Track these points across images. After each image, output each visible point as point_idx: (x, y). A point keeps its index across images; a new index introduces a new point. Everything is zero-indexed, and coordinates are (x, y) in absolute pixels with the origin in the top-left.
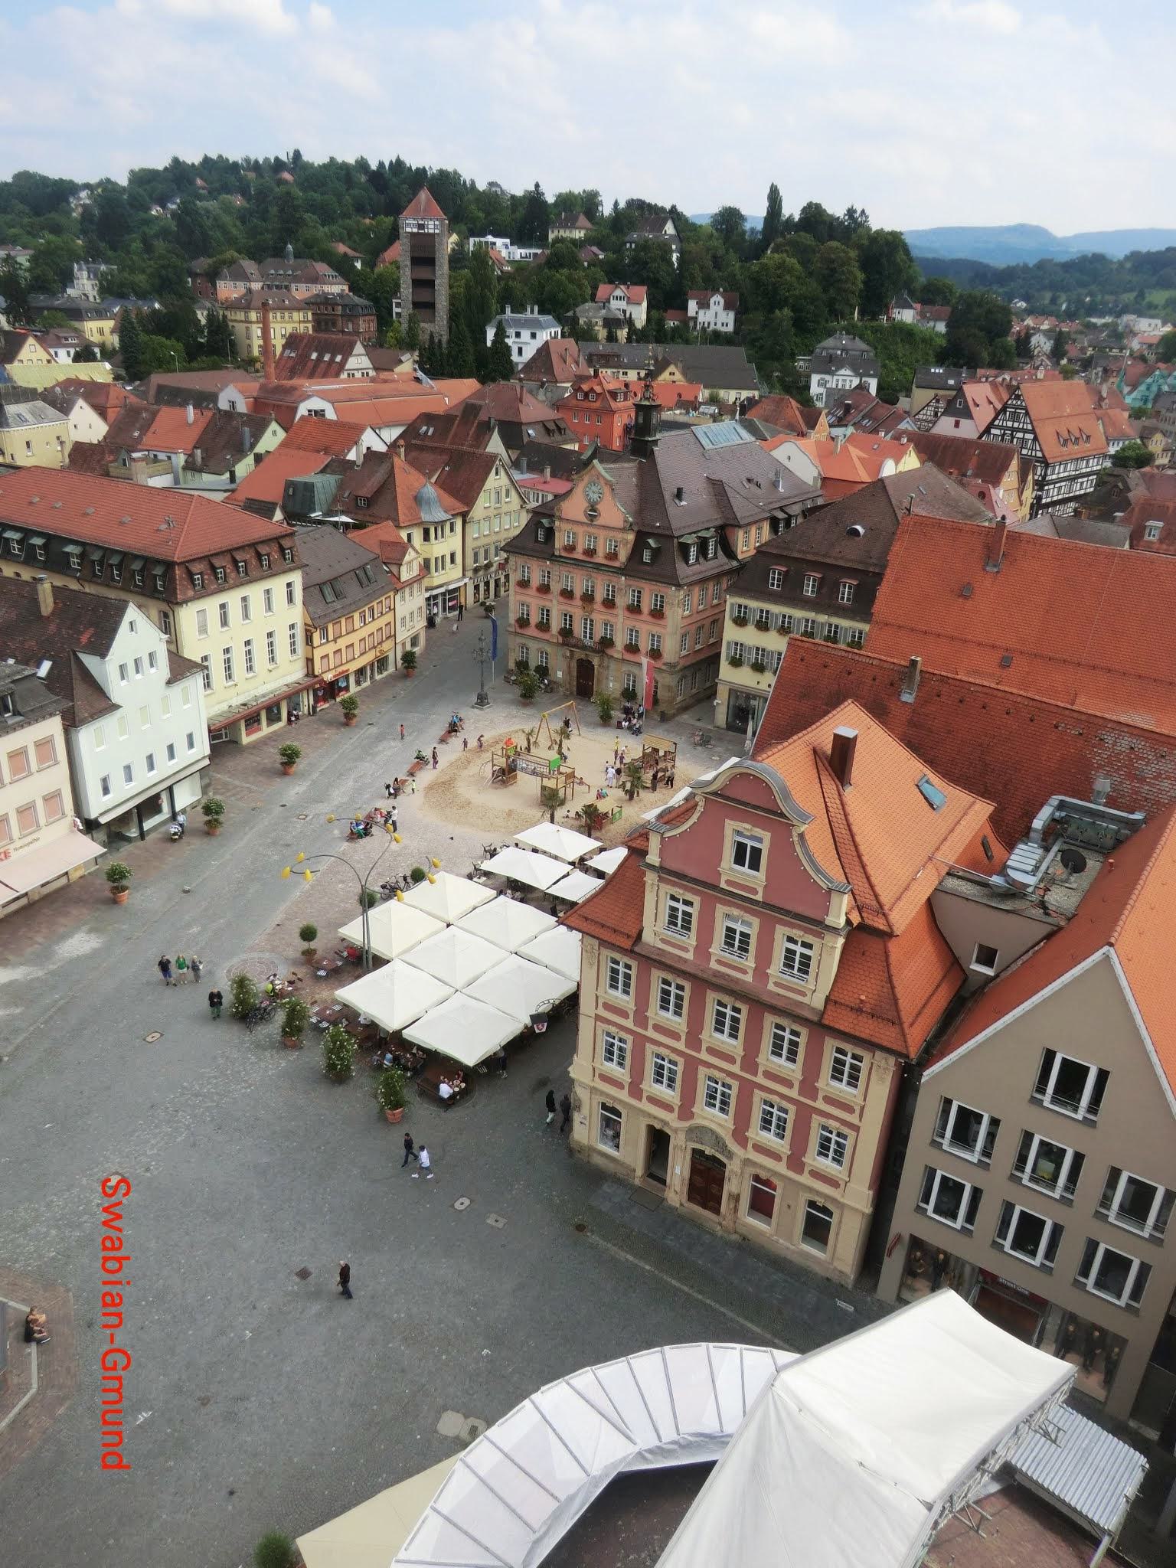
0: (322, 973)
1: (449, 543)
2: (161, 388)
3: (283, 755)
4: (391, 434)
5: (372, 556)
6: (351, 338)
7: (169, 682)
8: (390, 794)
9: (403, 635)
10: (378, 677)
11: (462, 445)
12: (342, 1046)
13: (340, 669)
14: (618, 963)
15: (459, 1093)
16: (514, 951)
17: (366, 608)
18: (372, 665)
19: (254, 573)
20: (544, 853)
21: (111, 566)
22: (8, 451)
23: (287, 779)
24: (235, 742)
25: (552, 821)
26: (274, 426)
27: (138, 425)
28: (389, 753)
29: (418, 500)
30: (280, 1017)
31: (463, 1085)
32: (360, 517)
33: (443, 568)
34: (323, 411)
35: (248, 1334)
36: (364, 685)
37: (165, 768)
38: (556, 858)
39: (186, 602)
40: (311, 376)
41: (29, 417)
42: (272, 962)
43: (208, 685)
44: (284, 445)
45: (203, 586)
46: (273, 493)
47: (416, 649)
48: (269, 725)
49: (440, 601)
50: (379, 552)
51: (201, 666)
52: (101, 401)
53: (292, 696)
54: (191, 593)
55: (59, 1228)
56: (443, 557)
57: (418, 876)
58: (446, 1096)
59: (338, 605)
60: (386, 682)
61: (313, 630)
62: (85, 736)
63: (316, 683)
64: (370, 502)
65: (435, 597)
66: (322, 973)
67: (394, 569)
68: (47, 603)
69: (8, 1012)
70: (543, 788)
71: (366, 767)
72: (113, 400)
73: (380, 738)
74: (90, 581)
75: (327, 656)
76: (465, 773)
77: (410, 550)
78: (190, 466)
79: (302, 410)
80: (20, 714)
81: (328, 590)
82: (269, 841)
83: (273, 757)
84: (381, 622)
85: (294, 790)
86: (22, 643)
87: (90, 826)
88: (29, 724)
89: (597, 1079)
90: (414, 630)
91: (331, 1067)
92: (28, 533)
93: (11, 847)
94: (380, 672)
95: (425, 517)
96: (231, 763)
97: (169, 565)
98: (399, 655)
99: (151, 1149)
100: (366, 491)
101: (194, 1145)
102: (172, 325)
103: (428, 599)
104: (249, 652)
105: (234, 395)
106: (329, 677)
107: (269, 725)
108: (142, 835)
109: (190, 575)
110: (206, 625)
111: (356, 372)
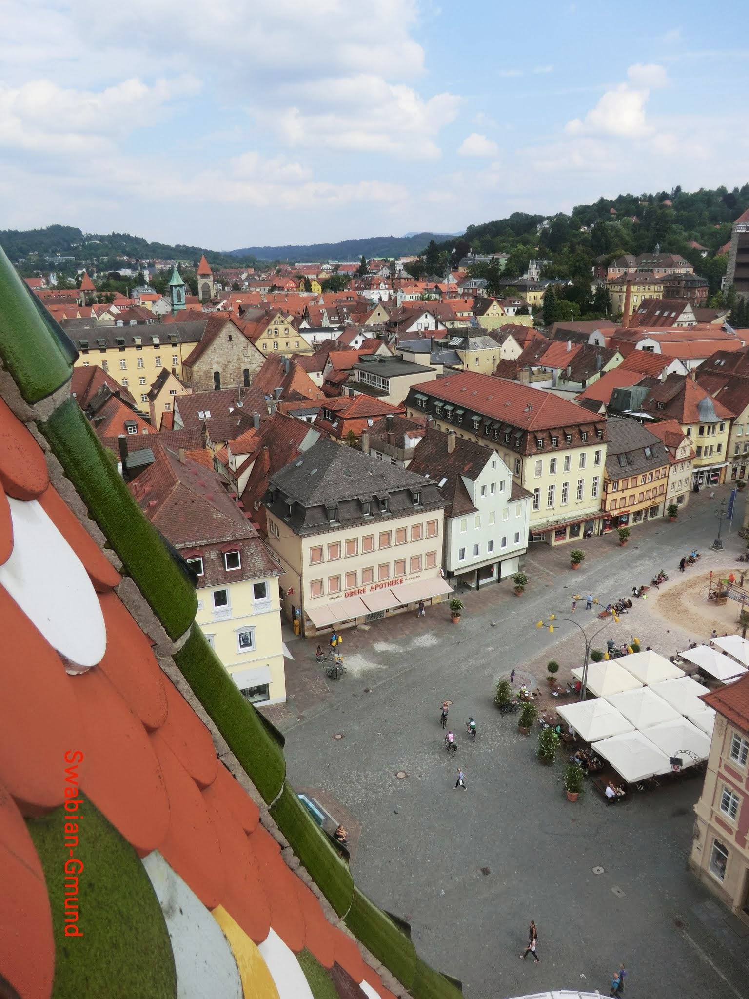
0: (556, 694)
1: (719, 437)
2: (559, 330)
3: (573, 556)
4: (695, 364)
5: (660, 441)
6: (684, 302)
7: (510, 500)
8: (635, 594)
9: (672, 494)
10: (649, 519)
11: (744, 374)
12: (550, 741)
13: (623, 510)
14: (740, 740)
15: (619, 797)
16: (685, 714)
17: (648, 473)
18: (646, 510)
19: (575, 443)
20: (732, 657)
21: (494, 430)
22: (466, 363)
23: (572, 572)
24: (547, 544)
25: (744, 636)
26: (618, 355)
27: (538, 351)
28: (642, 568)
29: (699, 407)
30: (520, 714)
31: (623, 793)
32: (658, 415)
33: (705, 455)
34: (653, 347)
35: (443, 892)
36: (639, 522)
37: (499, 550)
38: (739, 662)
39: (531, 455)
40: (654, 325)
41: (480, 345)
42: (529, 680)
43: (536, 506)
44: (621, 367)
45: (543, 447)
46: (604, 396)
47: (680, 506)
48: (570, 537)
49: (705, 475)
50: (663, 438)
51: (527, 494)
52: (522, 337)
53: (589, 521)
54: (534, 450)
55: (367, 789)
56: (712, 447)
57: (636, 649)
58: (609, 796)
59: (628, 469)
60: (654, 523)
61: (608, 482)
62: (456, 524)
63: (605, 516)
64: (666, 406)
65: (702, 473)
66: (556, 694)
67: (672, 450)
68: (452, 446)
69: (379, 666)
70: (743, 612)
71: (626, 574)
72: (529, 336)
73: (640, 557)
74: (482, 437)
75: (616, 500)
76: (691, 591)
77: (685, 439)
78: (564, 377)
79: (639, 346)
80: (422, 505)
81: (623, 459)
82: (550, 606)
83: (567, 558)
84: (657, 484)
85: (575, 580)
86: (435, 466)
87: (449, 575)
88: (426, 511)
89: (713, 819)
90: (681, 492)
91: (541, 753)
92: (456, 407)
93: (404, 578)
94: (652, 516)
95: (702, 419)
96: (542, 556)
97: (525, 432)
98: (667, 506)
99: (426, 765)
100: (665, 399)
101: (449, 771)
102: (570, 294)
103: (697, 473)
104: (565, 490)
105: (598, 336)
106: (615, 513)
107: (570, 537)
108: (478, 587)
109: (536, 439)
110: (541, 470)
111: (684, 323)
